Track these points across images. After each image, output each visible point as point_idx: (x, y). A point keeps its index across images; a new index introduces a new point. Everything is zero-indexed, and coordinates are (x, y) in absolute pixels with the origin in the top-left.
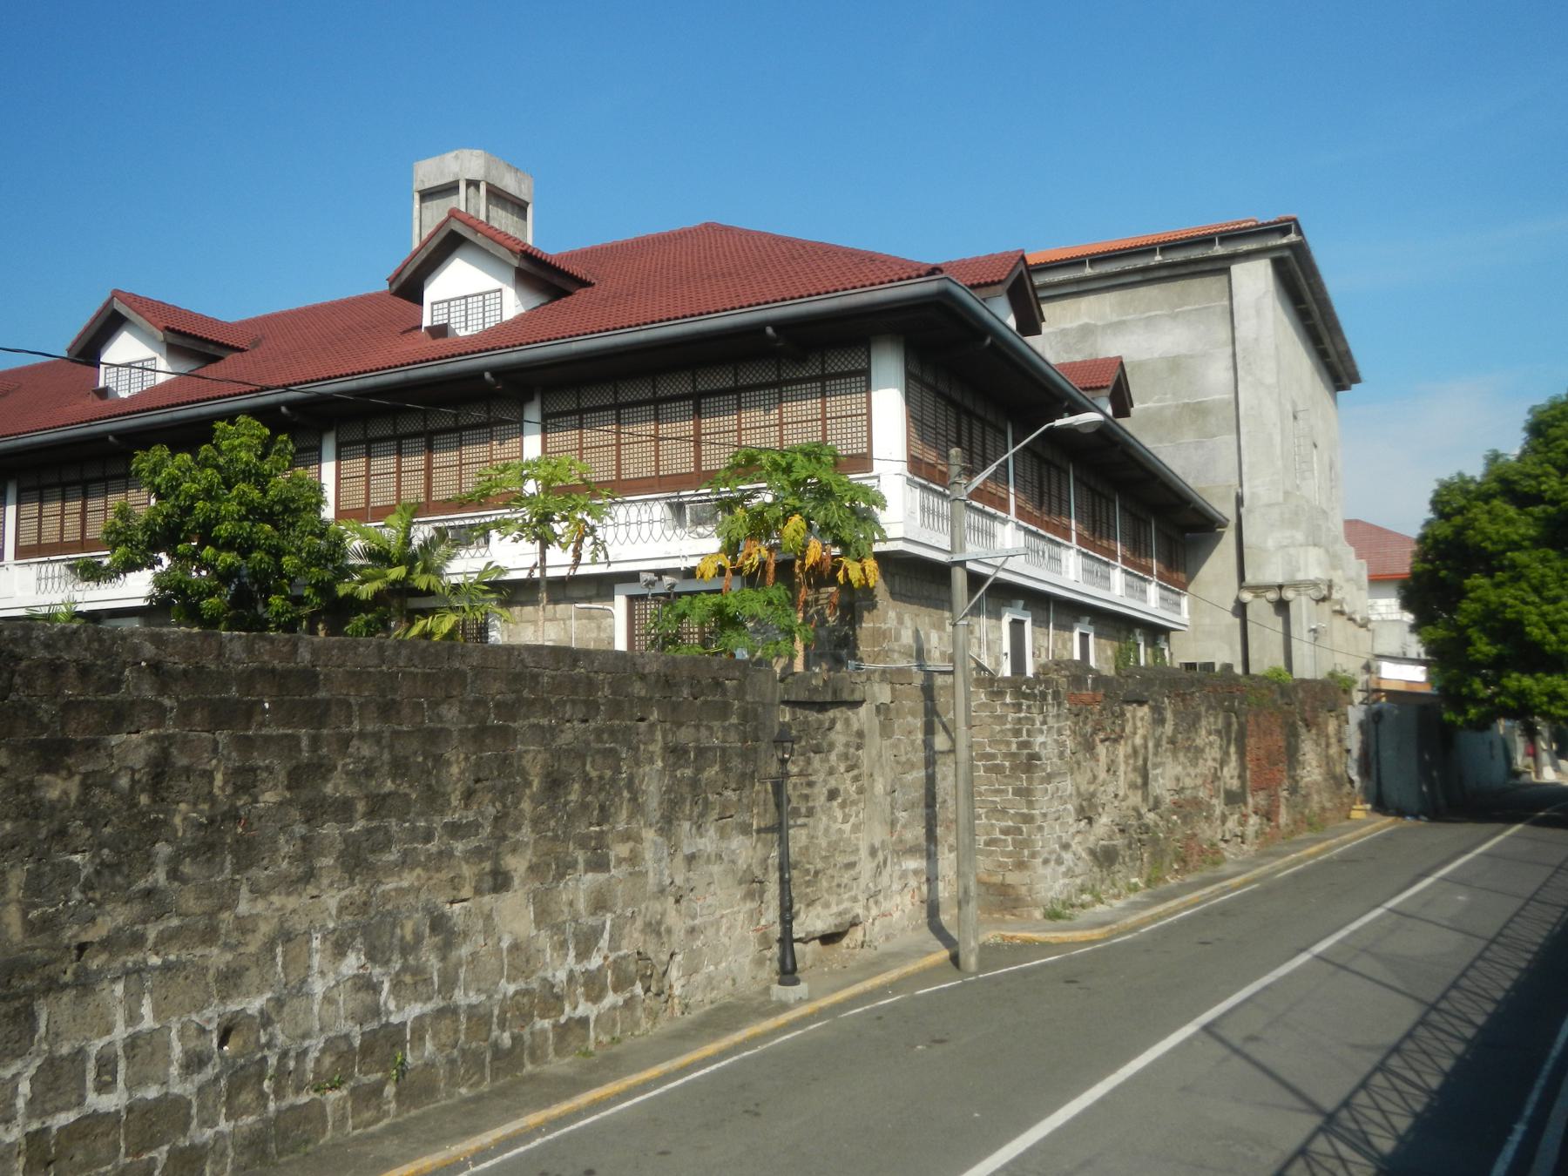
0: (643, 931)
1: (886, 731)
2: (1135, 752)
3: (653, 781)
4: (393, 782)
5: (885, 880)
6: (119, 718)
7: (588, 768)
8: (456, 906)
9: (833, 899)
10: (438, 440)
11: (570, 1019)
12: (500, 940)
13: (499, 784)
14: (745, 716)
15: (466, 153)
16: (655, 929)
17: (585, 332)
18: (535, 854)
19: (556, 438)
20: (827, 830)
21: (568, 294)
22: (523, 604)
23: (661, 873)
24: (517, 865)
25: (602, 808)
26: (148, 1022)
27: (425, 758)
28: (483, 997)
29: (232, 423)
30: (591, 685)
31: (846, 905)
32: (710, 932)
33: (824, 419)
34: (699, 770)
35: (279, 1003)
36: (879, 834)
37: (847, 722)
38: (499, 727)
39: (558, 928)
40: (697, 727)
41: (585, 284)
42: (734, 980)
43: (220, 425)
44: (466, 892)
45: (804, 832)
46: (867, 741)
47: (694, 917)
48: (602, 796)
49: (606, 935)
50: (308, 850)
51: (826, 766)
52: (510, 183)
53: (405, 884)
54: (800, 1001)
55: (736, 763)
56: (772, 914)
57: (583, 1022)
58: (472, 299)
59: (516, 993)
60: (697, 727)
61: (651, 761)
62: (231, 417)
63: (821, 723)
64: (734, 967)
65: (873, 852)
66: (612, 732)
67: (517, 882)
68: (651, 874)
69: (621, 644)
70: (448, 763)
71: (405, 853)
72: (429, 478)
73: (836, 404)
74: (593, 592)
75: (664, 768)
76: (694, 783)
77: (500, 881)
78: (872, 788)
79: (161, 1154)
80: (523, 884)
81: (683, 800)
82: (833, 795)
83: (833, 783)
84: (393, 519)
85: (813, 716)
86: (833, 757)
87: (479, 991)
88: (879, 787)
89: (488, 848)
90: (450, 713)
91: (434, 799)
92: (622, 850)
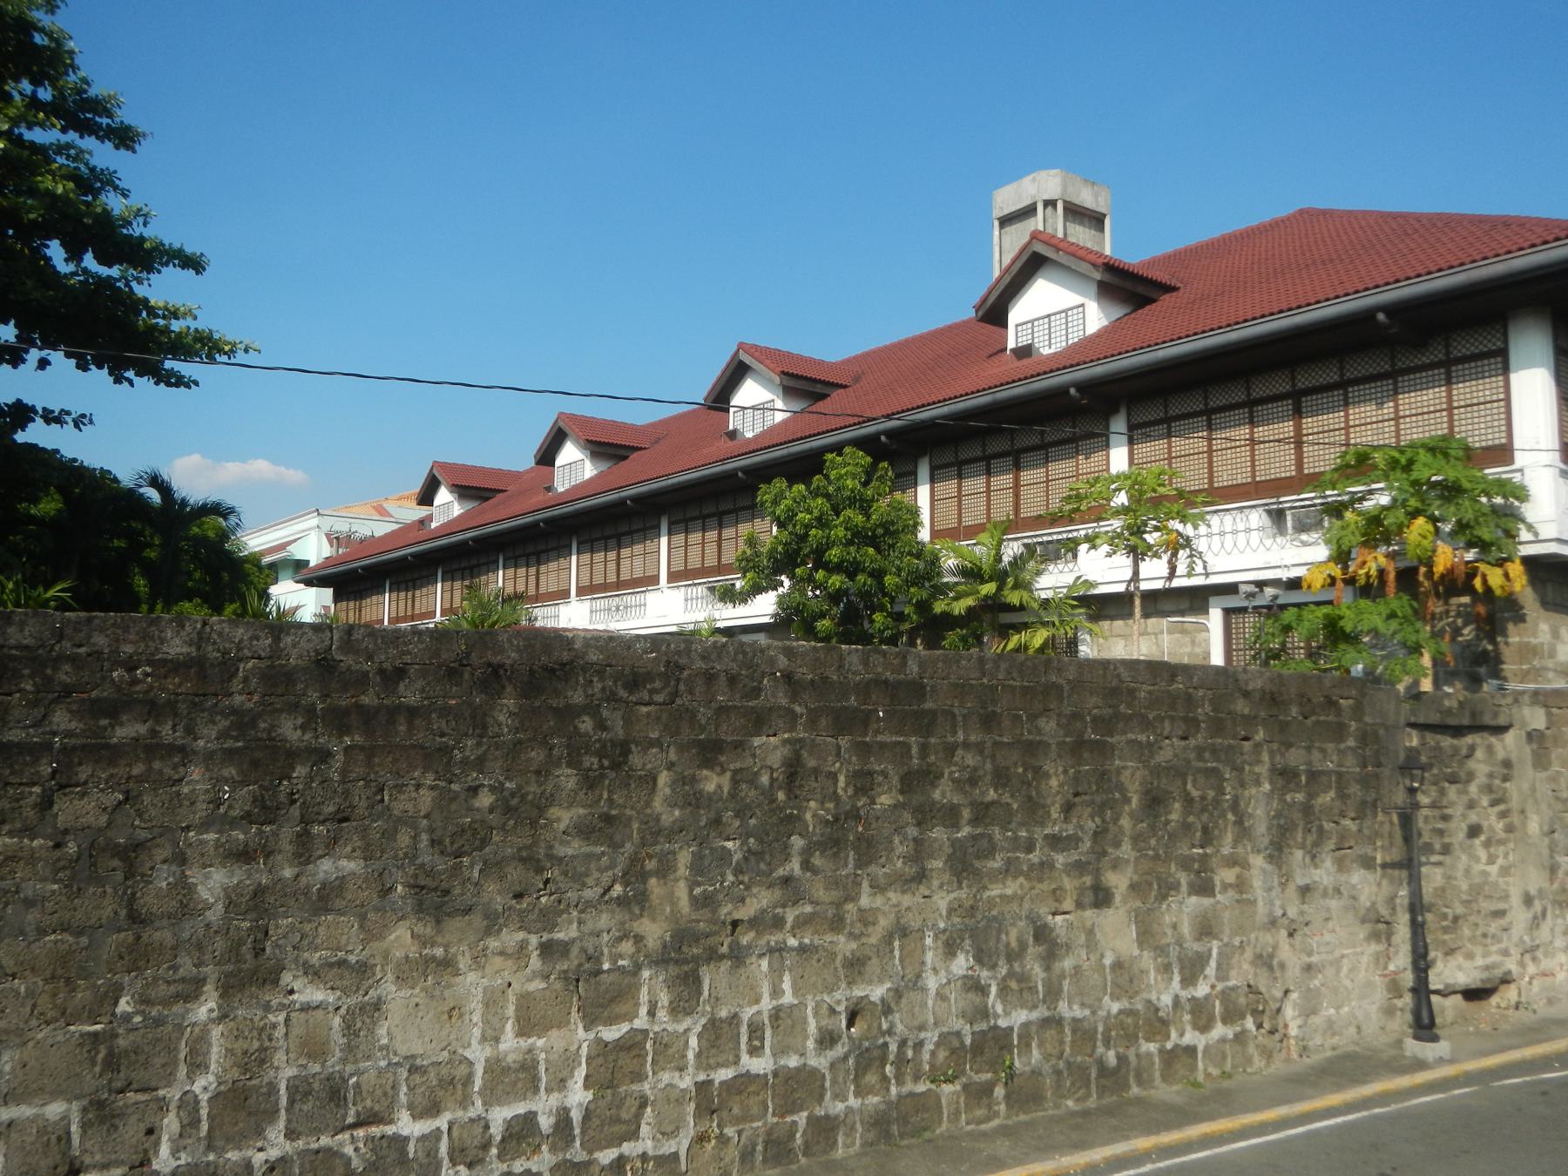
0: (1253, 963)
1: (1541, 761)
3: (1260, 804)
4: (996, 791)
5: (1544, 933)
6: (759, 722)
7: (1189, 786)
8: (1059, 918)
9: (1478, 950)
10: (1024, 458)
11: (1177, 1046)
12: (1102, 956)
13: (1098, 799)
14: (1364, 738)
15: (1043, 175)
16: (1265, 961)
17: (1173, 337)
18: (1136, 872)
19: (1146, 449)
20: (1467, 871)
21: (1151, 301)
22: (1112, 618)
23: (1272, 903)
24: (1118, 881)
25: (1205, 830)
26: (788, 998)
27: (1025, 770)
28: (1087, 1012)
29: (840, 454)
30: (1189, 700)
31: (1495, 958)
32: (1330, 972)
33: (1450, 409)
34: (1311, 796)
35: (898, 993)
36: (1535, 880)
37: (1490, 749)
38: (1097, 741)
39: (1161, 950)
40: (1309, 749)
41: (1169, 289)
42: (1358, 1027)
43: (829, 456)
44: (1068, 904)
45: (1438, 871)
46: (1516, 772)
47: (1310, 954)
48: (1205, 817)
49: (1213, 963)
50: (919, 853)
51: (1465, 799)
52: (1087, 198)
53: (1009, 892)
54: (1441, 1061)
55: (1354, 789)
56: (1401, 960)
57: (1191, 1051)
58: (1058, 317)
59: (1121, 1012)
60: (1309, 749)
61: (1258, 783)
62: (838, 448)
63: (1456, 750)
64: (1359, 1014)
65: (1528, 901)
66: (1214, 751)
67: (1118, 899)
68: (1260, 903)
69: (1217, 659)
70: (1047, 776)
71: (1009, 862)
72: (1017, 496)
73: (1464, 391)
74: (1185, 605)
75: (1272, 791)
76: (1307, 810)
77: (1101, 897)
78: (1524, 825)
79: (801, 1118)
80: (1124, 902)
81: (1295, 826)
82: (1474, 831)
83: (1473, 818)
84: (984, 537)
85: (1447, 742)
86: (1473, 788)
87: (1083, 1005)
88: (1534, 826)
89: (1089, 863)
90: (1048, 726)
91: (1035, 810)
92: (1228, 875)
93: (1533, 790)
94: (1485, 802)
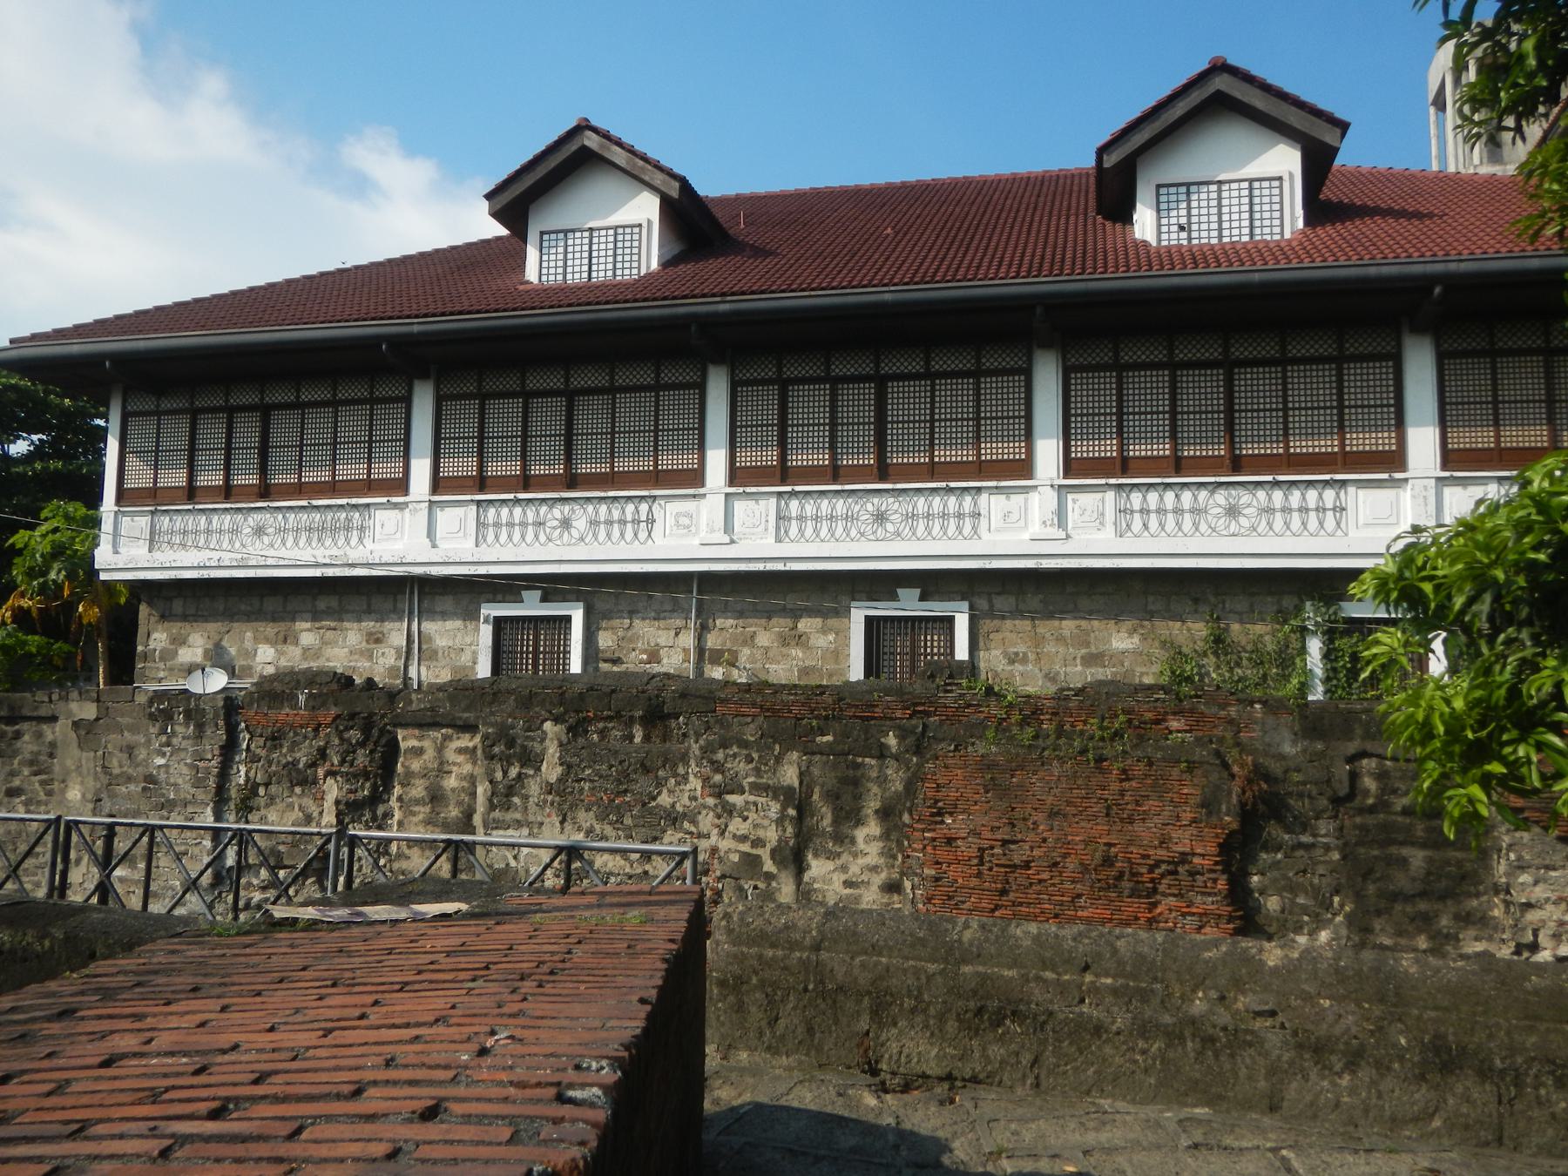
2: (436, 797)
37: (39, 735)
46: (59, 752)
51: (8, 768)
78: (63, 791)
83: (17, 782)
93: (79, 767)
94: (26, 772)
